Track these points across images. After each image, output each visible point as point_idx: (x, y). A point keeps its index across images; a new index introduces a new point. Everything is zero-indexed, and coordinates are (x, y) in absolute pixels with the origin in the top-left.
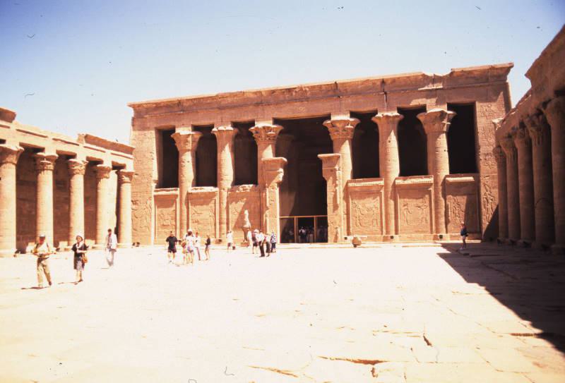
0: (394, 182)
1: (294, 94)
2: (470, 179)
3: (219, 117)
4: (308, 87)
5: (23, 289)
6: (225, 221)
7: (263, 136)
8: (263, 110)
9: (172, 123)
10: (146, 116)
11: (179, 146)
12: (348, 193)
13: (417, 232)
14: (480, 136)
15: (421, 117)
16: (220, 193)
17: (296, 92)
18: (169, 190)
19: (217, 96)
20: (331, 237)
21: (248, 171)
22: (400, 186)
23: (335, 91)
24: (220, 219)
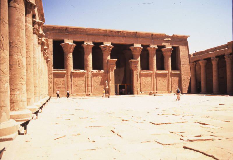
0: (156, 72)
1: (120, 33)
2: (179, 72)
3: (87, 38)
4: (126, 32)
5: (159, 115)
6: (90, 86)
7: (108, 50)
8: (107, 38)
9: (62, 38)
10: (47, 32)
11: (65, 50)
12: (141, 75)
13: (163, 90)
14: (181, 58)
15: (163, 50)
16: (87, 73)
17: (120, 33)
18: (62, 71)
19: (87, 29)
20: (135, 92)
21: (98, 64)
22: (158, 73)
23: (136, 36)
24: (88, 84)
